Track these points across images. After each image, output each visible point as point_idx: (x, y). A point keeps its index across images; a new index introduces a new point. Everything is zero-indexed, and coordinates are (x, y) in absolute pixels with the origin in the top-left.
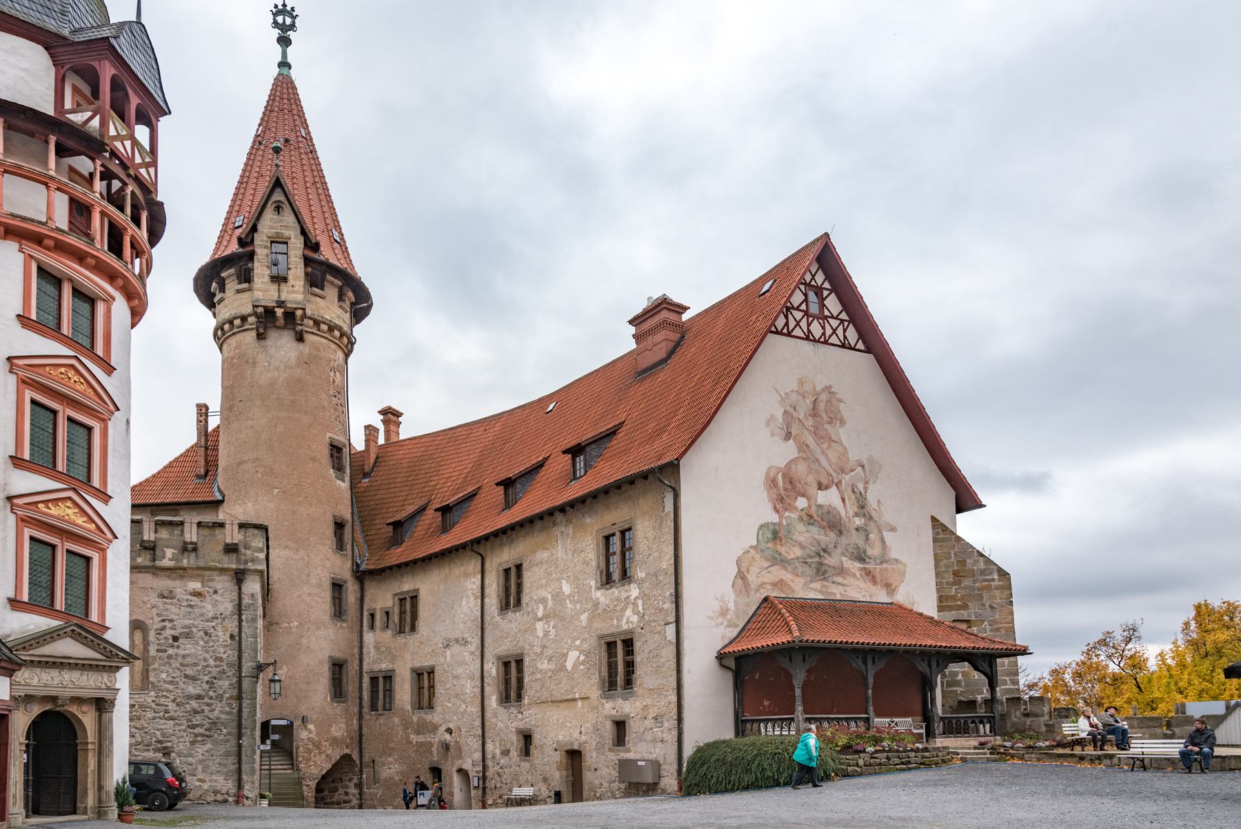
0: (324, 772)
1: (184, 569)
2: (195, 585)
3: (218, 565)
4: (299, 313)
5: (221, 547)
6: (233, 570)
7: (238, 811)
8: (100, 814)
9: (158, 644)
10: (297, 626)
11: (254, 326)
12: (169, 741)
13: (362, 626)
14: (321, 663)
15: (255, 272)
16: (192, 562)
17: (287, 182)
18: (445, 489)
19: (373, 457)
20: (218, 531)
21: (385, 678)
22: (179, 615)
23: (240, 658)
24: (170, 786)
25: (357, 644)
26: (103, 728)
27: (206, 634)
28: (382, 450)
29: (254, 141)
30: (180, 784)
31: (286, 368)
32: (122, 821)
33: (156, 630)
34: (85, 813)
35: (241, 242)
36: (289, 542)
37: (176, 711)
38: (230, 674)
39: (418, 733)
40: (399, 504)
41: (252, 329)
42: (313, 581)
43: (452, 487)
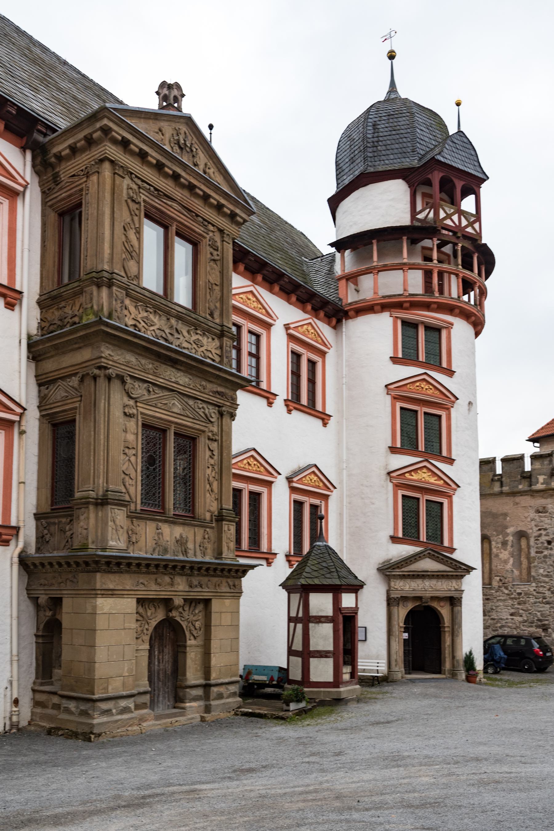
8: (453, 675)
9: (537, 548)
12: (547, 620)
26: (454, 617)
33: (535, 537)
34: (444, 674)
37: (551, 597)
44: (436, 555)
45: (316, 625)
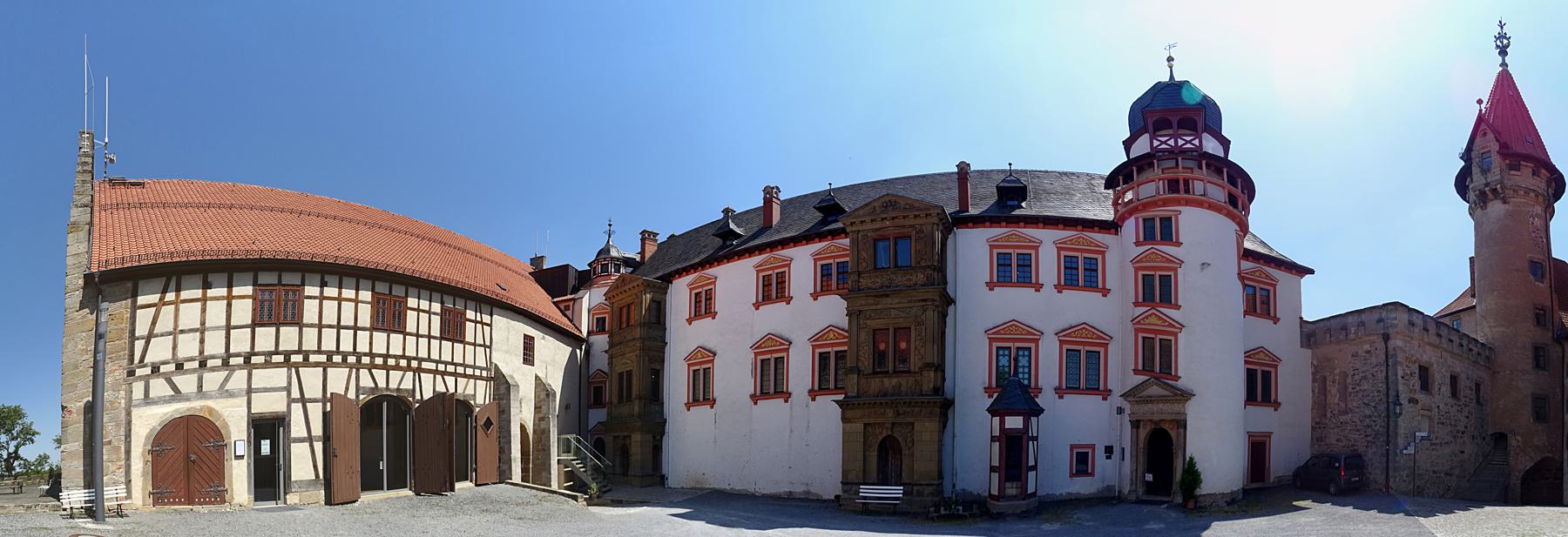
23: (1388, 389)
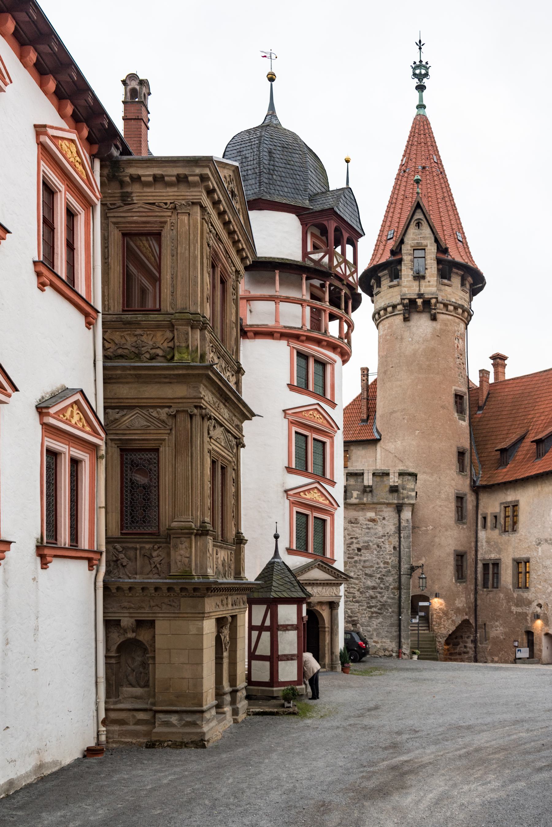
0: (450, 632)
1: (364, 504)
2: (371, 514)
3: (385, 501)
4: (433, 301)
5: (387, 489)
6: (395, 504)
7: (401, 663)
9: (349, 554)
10: (432, 529)
11: (402, 312)
12: (356, 617)
13: (477, 526)
14: (448, 555)
15: (403, 273)
16: (369, 499)
17: (424, 203)
18: (540, 422)
19: (485, 393)
20: (385, 478)
21: (493, 564)
22: (361, 534)
23: (400, 562)
24: (359, 646)
25: (473, 539)
27: (378, 546)
28: (492, 388)
29: (400, 170)
30: (366, 646)
31: (424, 341)
32: (344, 672)
35: (393, 253)
36: (426, 469)
37: (360, 597)
38: (393, 572)
39: (517, 605)
40: (504, 432)
41: (400, 314)
42: (443, 496)
43: (544, 421)
44: (324, 565)
45: (284, 632)
